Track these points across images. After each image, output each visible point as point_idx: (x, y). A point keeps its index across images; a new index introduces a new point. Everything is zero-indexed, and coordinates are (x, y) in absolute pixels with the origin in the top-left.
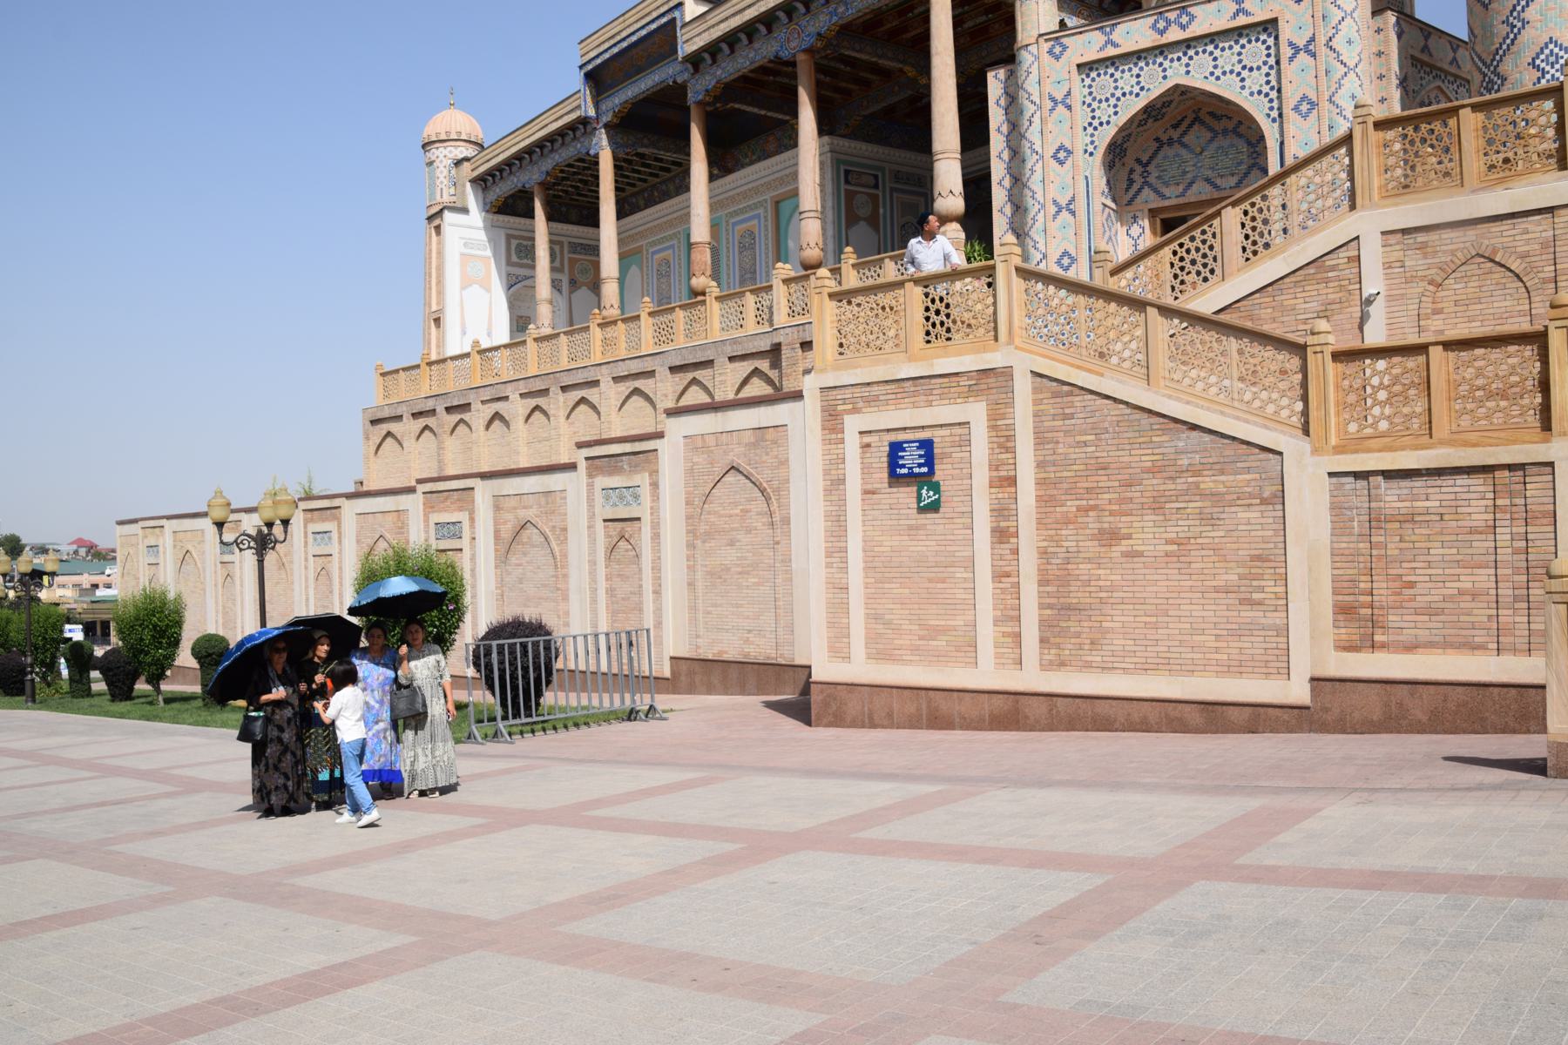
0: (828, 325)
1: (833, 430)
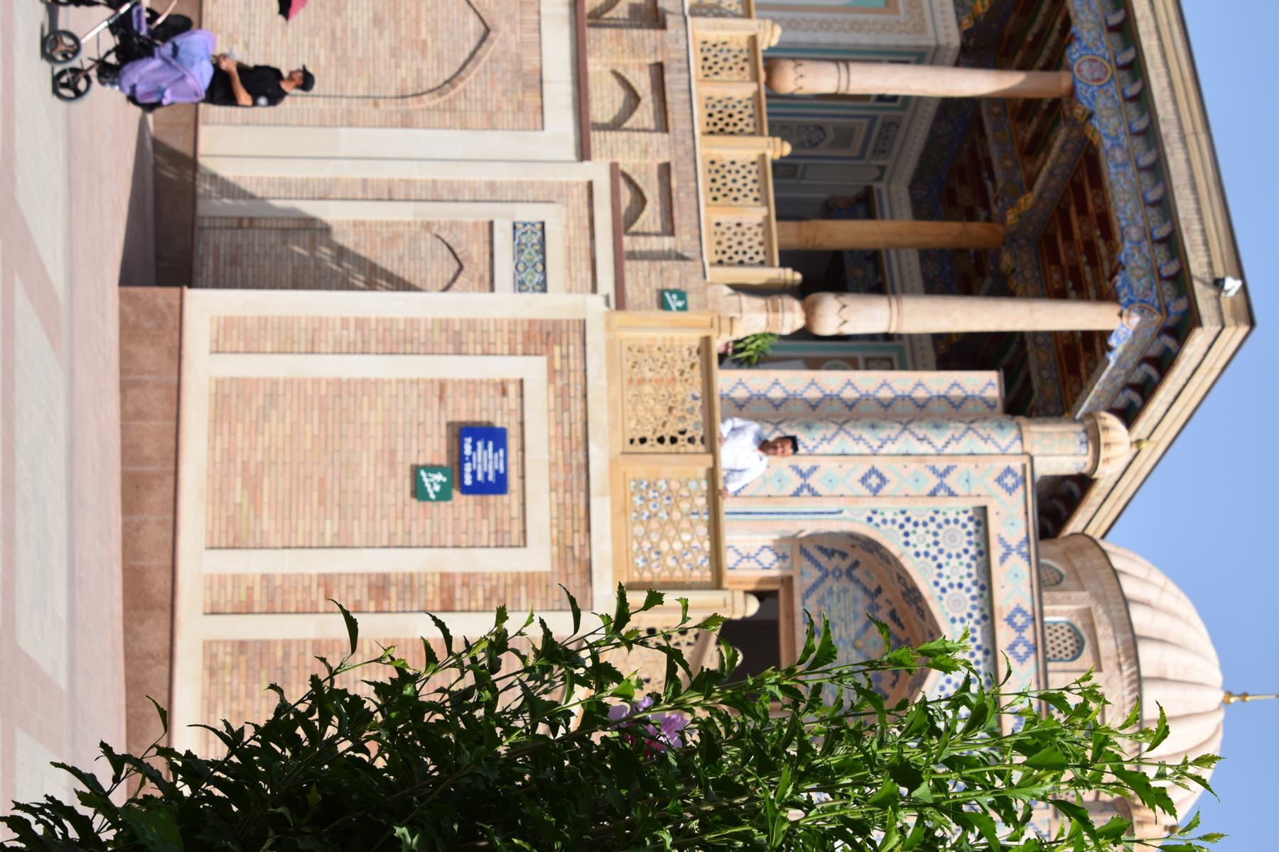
0: (668, 334)
1: (528, 337)
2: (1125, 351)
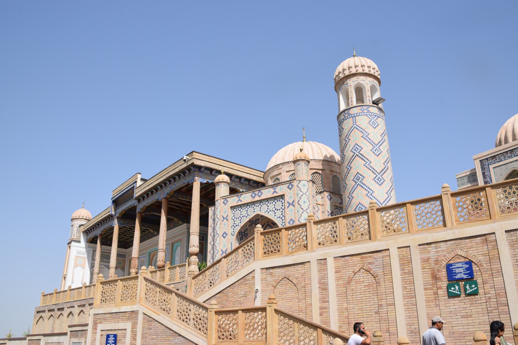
2: (208, 179)
